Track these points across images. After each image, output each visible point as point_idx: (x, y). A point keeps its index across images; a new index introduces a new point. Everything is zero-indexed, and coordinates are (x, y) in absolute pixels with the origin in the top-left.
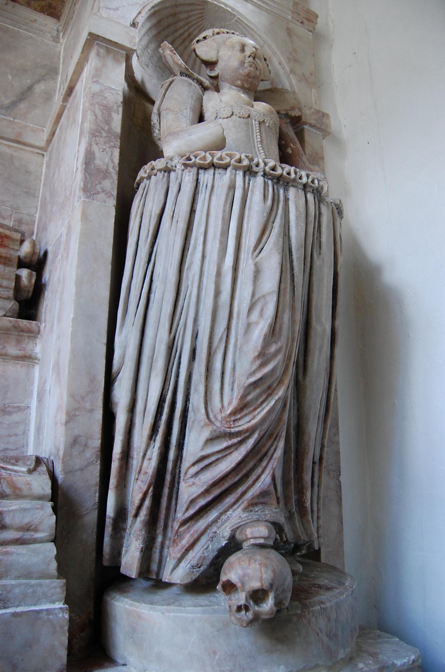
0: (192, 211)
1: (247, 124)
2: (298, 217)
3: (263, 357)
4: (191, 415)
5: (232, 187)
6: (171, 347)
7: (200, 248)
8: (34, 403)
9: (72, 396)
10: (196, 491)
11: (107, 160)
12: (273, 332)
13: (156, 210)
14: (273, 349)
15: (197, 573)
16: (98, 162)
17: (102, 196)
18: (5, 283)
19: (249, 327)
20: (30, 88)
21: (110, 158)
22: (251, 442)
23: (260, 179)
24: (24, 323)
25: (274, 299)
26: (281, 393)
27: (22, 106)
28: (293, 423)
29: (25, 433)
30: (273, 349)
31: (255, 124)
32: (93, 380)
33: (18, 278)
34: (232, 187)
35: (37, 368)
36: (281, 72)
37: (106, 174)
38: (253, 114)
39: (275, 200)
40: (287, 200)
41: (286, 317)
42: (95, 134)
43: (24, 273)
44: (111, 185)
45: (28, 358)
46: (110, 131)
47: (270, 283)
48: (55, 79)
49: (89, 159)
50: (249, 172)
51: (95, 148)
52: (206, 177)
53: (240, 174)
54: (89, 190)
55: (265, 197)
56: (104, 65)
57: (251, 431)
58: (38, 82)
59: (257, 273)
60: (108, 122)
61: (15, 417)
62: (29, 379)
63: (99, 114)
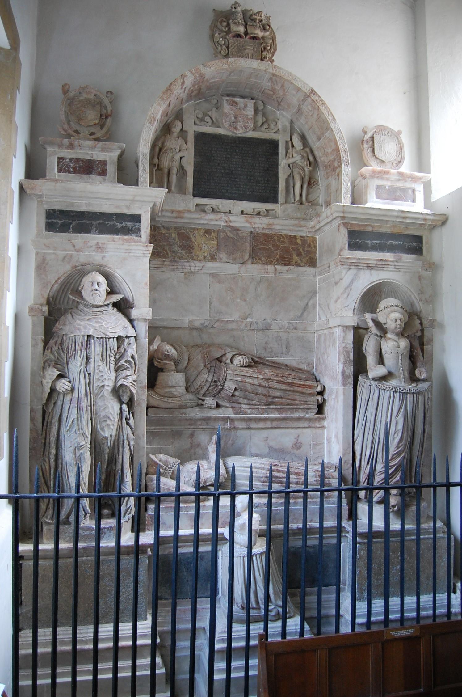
0: (378, 402)
1: (397, 356)
2: (410, 404)
3: (398, 447)
4: (378, 459)
5: (390, 397)
6: (372, 441)
7: (380, 414)
8: (326, 442)
9: (344, 449)
10: (379, 479)
11: (349, 372)
12: (401, 440)
13: (367, 399)
14: (401, 445)
15: (380, 499)
16: (346, 373)
17: (349, 385)
18: (314, 403)
19: (394, 439)
20: (307, 304)
21: (350, 371)
22: (394, 468)
23: (398, 394)
24: (321, 416)
25: (401, 431)
26: (403, 455)
27: (305, 314)
28: (409, 458)
29: (324, 451)
30: (401, 445)
31: (400, 355)
32: (349, 444)
33: (318, 400)
34: (390, 397)
35: (326, 430)
36: (416, 301)
37: (349, 377)
38: (399, 352)
39: (403, 400)
40: (407, 398)
41: (405, 435)
42: (345, 363)
43: (319, 398)
44: (351, 380)
45: (323, 427)
46: (349, 360)
47: (400, 426)
48: (316, 296)
49: (344, 372)
50: (395, 392)
51: (345, 368)
52: (382, 392)
53: (392, 393)
54: (344, 385)
55: (399, 400)
56: (346, 334)
57: (394, 465)
58: (310, 300)
59: (397, 423)
60: (349, 357)
61: (320, 446)
62: (323, 434)
63: (345, 354)
